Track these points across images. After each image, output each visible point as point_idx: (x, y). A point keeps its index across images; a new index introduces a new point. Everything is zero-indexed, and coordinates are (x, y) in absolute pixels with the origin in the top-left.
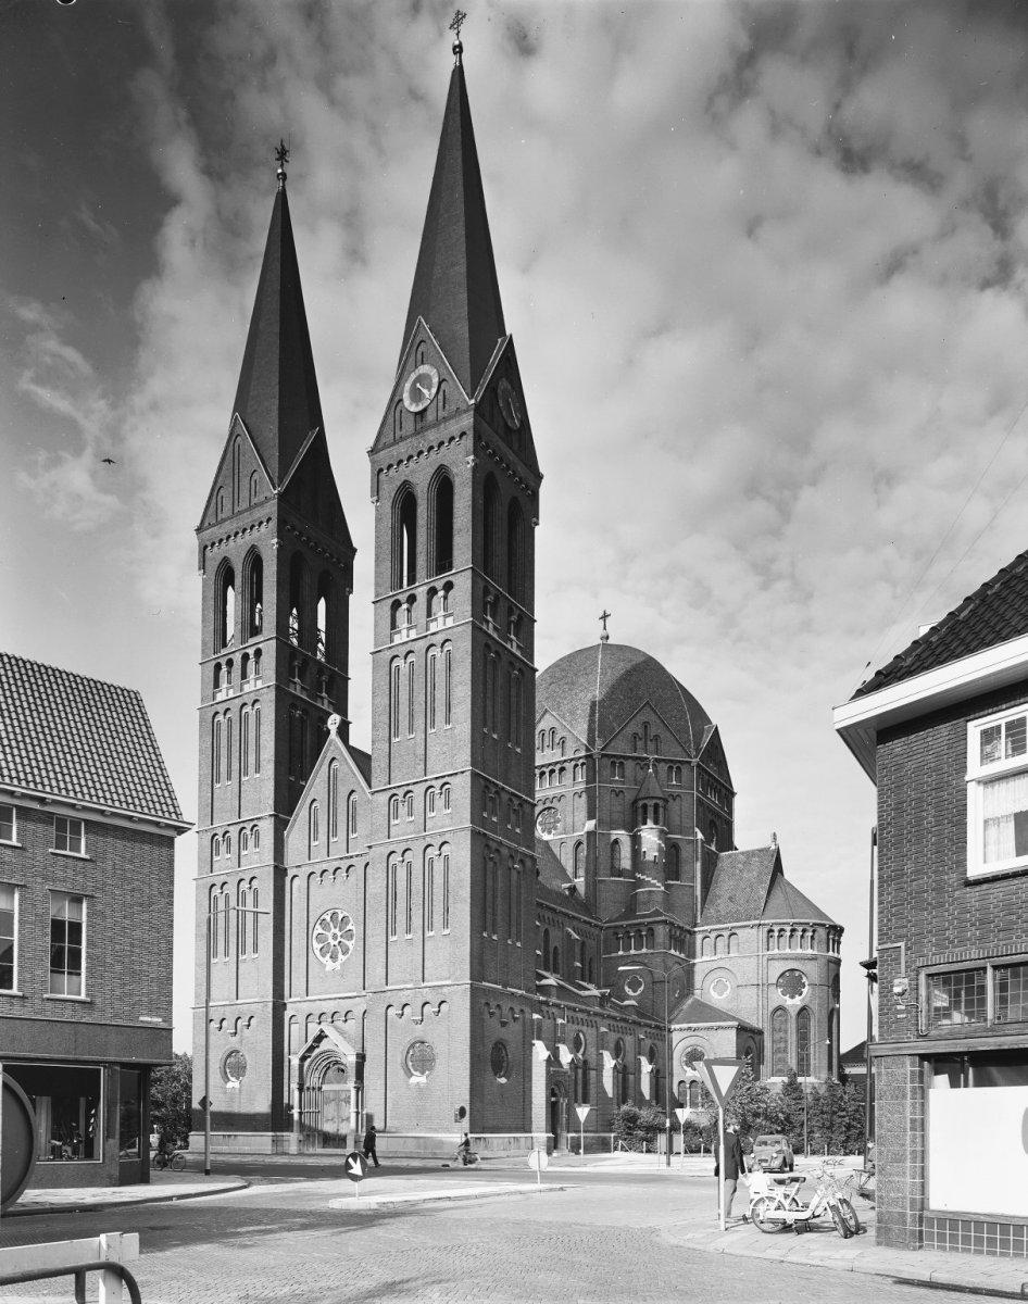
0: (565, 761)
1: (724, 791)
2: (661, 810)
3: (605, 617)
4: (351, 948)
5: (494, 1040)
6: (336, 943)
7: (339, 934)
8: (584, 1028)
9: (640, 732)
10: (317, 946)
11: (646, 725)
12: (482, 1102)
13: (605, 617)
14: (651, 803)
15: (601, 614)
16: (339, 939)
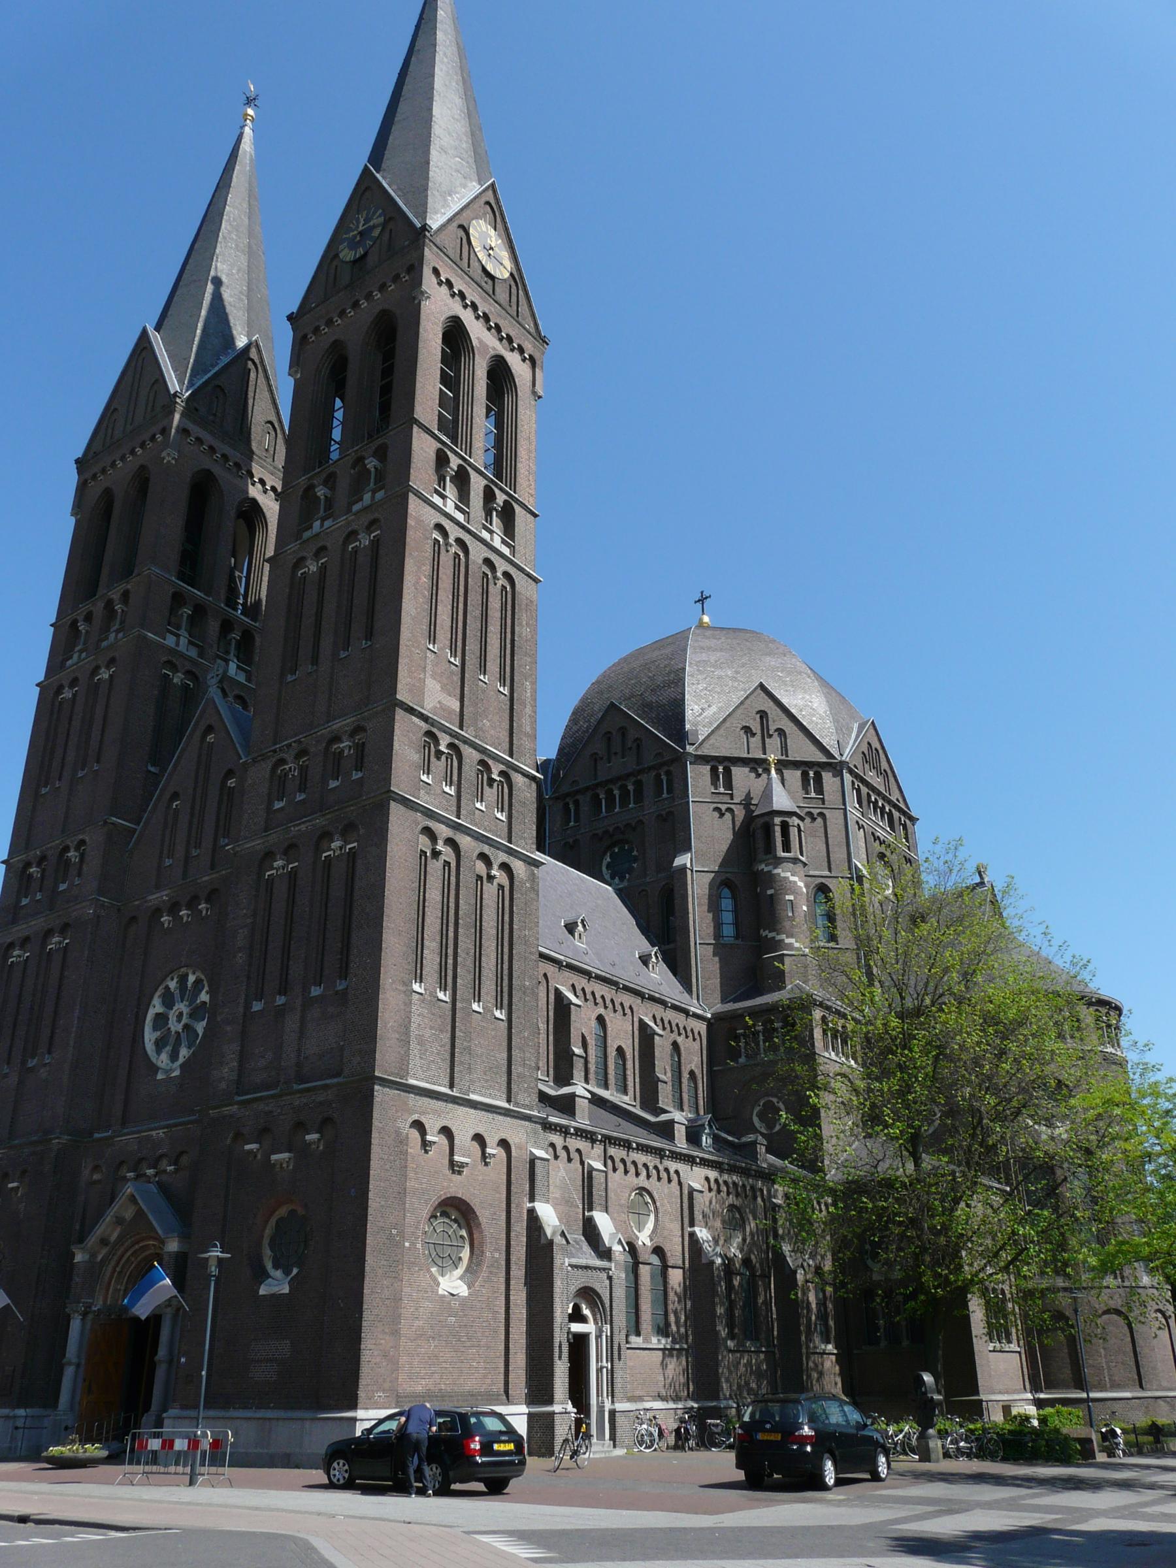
0: (640, 772)
1: (896, 814)
2: (793, 832)
3: (702, 600)
4: (200, 1031)
5: (434, 1200)
6: (179, 1028)
8: (652, 1185)
9: (756, 728)
10: (150, 1037)
11: (763, 715)
12: (396, 1333)
13: (702, 600)
14: (777, 820)
15: (698, 597)
16: (185, 1020)
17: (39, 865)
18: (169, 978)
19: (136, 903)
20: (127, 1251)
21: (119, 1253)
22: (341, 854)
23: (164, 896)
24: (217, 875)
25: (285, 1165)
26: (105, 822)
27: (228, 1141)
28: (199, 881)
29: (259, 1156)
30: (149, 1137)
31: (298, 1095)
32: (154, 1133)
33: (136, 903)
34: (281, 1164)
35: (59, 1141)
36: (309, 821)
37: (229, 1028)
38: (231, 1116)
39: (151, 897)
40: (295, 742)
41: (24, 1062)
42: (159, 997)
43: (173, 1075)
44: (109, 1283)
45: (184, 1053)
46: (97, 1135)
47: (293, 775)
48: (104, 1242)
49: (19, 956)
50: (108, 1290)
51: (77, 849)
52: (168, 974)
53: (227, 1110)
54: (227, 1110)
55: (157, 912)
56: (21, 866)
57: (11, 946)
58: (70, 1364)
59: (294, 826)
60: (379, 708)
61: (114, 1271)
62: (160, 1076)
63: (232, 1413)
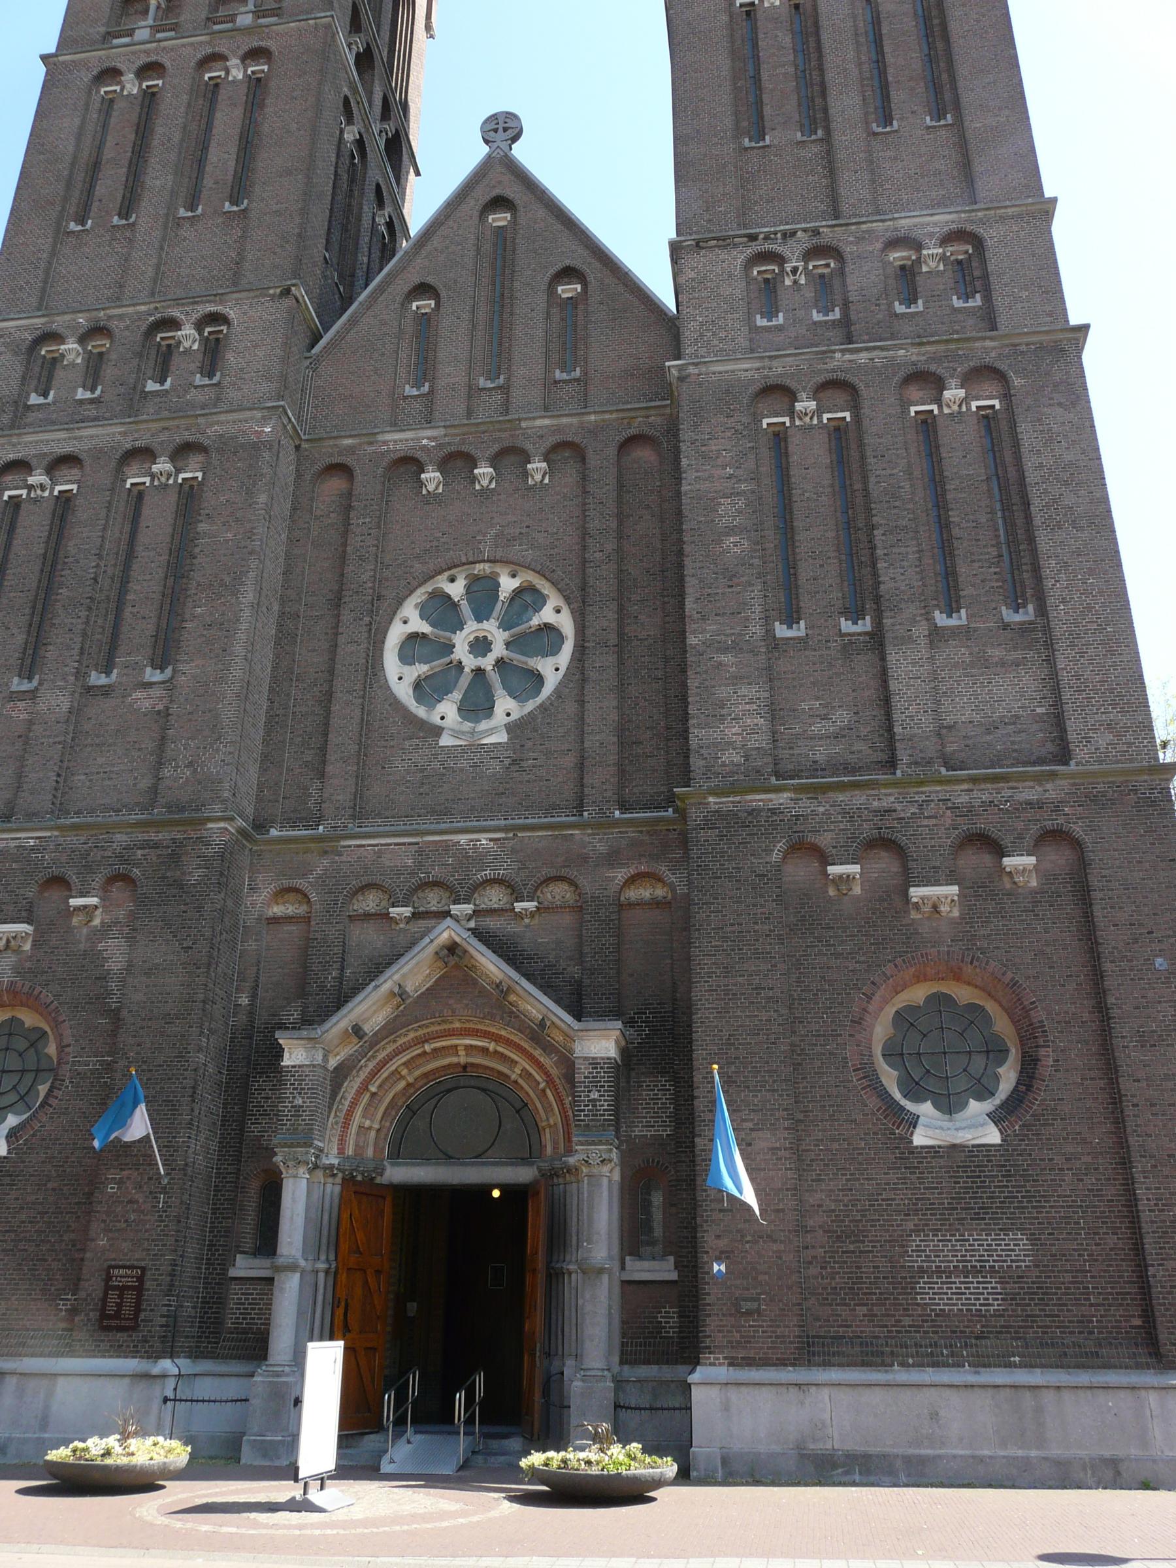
7: (498, 650)
17: (82, 340)
18: (447, 574)
19: (348, 442)
20: (397, 1053)
21: (381, 1056)
22: (959, 413)
23: (425, 438)
24: (575, 420)
25: (944, 909)
26: (287, 292)
27: (775, 857)
28: (524, 424)
29: (857, 890)
30: (447, 847)
31: (965, 786)
32: (463, 839)
33: (348, 442)
34: (935, 907)
35: (220, 829)
36: (881, 348)
37: (725, 658)
38: (773, 811)
39: (388, 437)
40: (805, 230)
41: (81, 675)
42: (416, 606)
43: (485, 741)
44: (350, 1113)
45: (506, 707)
46: (274, 832)
47: (795, 282)
48: (357, 1031)
49: (42, 487)
50: (346, 1125)
51: (199, 326)
52: (450, 568)
53: (756, 800)
54: (756, 800)
55: (410, 464)
56: (29, 337)
57: (21, 466)
58: (293, 1268)
59: (843, 351)
60: (1010, 211)
61: (364, 1087)
62: (446, 741)
63: (900, 1375)
